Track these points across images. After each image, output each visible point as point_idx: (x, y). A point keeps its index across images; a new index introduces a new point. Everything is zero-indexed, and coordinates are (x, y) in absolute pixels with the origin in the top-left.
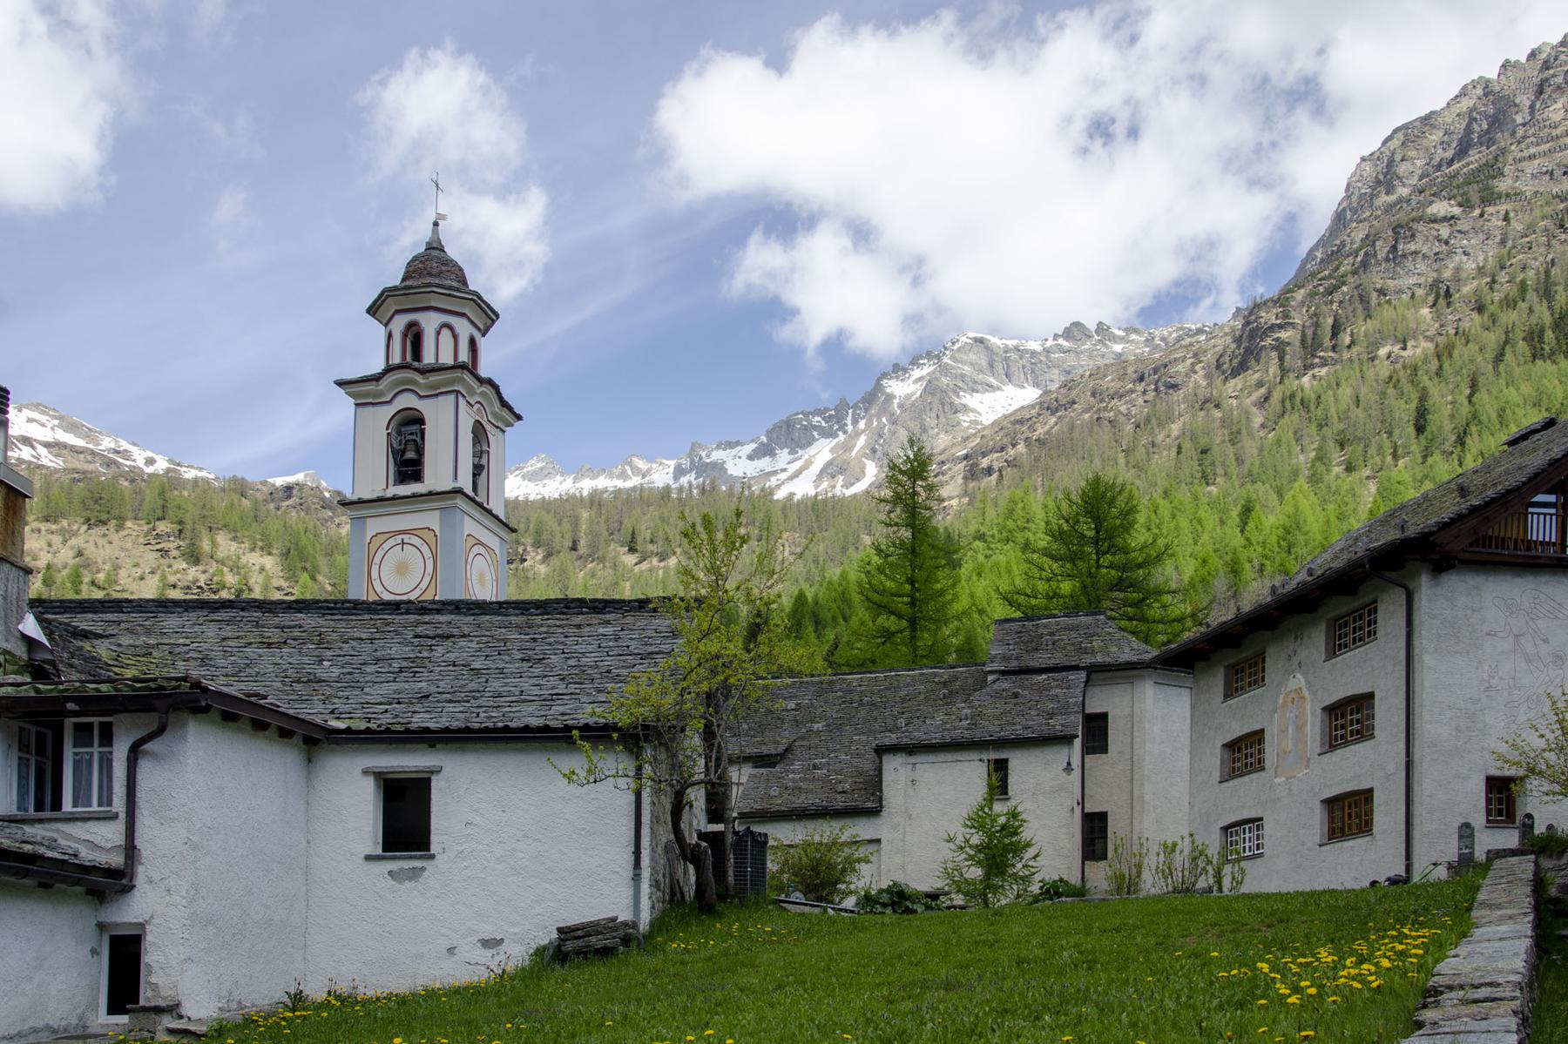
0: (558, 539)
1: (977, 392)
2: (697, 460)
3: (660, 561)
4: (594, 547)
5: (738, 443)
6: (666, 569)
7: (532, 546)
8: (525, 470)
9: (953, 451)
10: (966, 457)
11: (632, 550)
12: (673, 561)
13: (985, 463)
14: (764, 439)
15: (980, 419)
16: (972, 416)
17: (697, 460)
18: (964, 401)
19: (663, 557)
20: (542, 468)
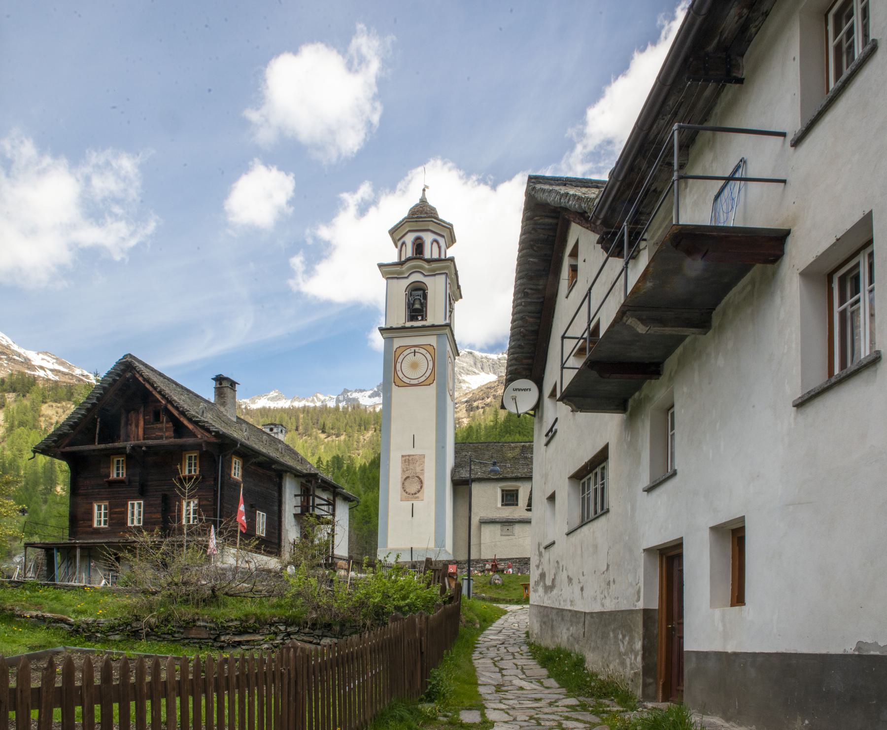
0: (290, 425)
2: (346, 396)
3: (336, 437)
4: (306, 430)
5: (364, 390)
6: (340, 441)
8: (269, 396)
9: (460, 399)
10: (466, 402)
11: (323, 432)
12: (342, 438)
13: (475, 404)
14: (376, 389)
15: (470, 386)
16: (467, 385)
17: (346, 396)
19: (338, 436)
20: (276, 396)
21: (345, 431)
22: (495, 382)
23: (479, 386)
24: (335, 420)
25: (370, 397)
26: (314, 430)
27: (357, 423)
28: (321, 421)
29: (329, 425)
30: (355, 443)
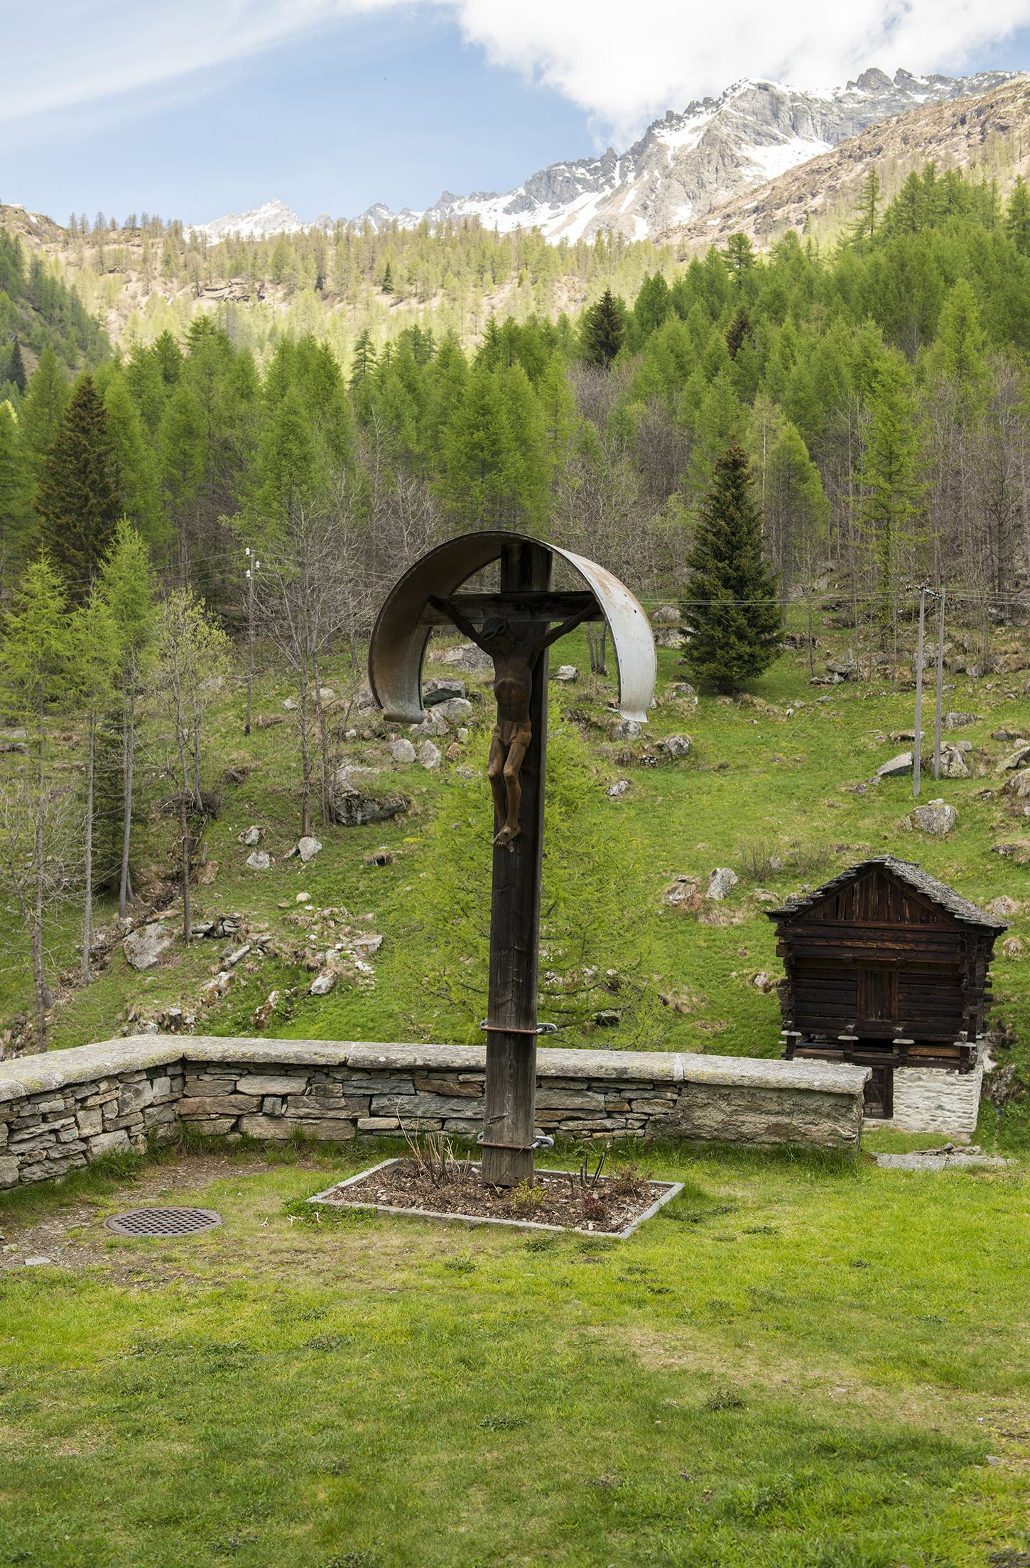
1: (761, 144)
2: (448, 211)
4: (342, 284)
5: (493, 195)
6: (428, 312)
7: (271, 281)
8: (257, 217)
9: (740, 204)
10: (756, 210)
11: (386, 290)
12: (435, 303)
14: (522, 191)
15: (764, 174)
16: (755, 170)
18: (746, 154)
20: (276, 216)
22: (832, 156)
23: (790, 167)
24: (418, 258)
25: (507, 211)
26: (363, 286)
27: (474, 265)
28: (381, 263)
29: (400, 270)
30: (469, 316)
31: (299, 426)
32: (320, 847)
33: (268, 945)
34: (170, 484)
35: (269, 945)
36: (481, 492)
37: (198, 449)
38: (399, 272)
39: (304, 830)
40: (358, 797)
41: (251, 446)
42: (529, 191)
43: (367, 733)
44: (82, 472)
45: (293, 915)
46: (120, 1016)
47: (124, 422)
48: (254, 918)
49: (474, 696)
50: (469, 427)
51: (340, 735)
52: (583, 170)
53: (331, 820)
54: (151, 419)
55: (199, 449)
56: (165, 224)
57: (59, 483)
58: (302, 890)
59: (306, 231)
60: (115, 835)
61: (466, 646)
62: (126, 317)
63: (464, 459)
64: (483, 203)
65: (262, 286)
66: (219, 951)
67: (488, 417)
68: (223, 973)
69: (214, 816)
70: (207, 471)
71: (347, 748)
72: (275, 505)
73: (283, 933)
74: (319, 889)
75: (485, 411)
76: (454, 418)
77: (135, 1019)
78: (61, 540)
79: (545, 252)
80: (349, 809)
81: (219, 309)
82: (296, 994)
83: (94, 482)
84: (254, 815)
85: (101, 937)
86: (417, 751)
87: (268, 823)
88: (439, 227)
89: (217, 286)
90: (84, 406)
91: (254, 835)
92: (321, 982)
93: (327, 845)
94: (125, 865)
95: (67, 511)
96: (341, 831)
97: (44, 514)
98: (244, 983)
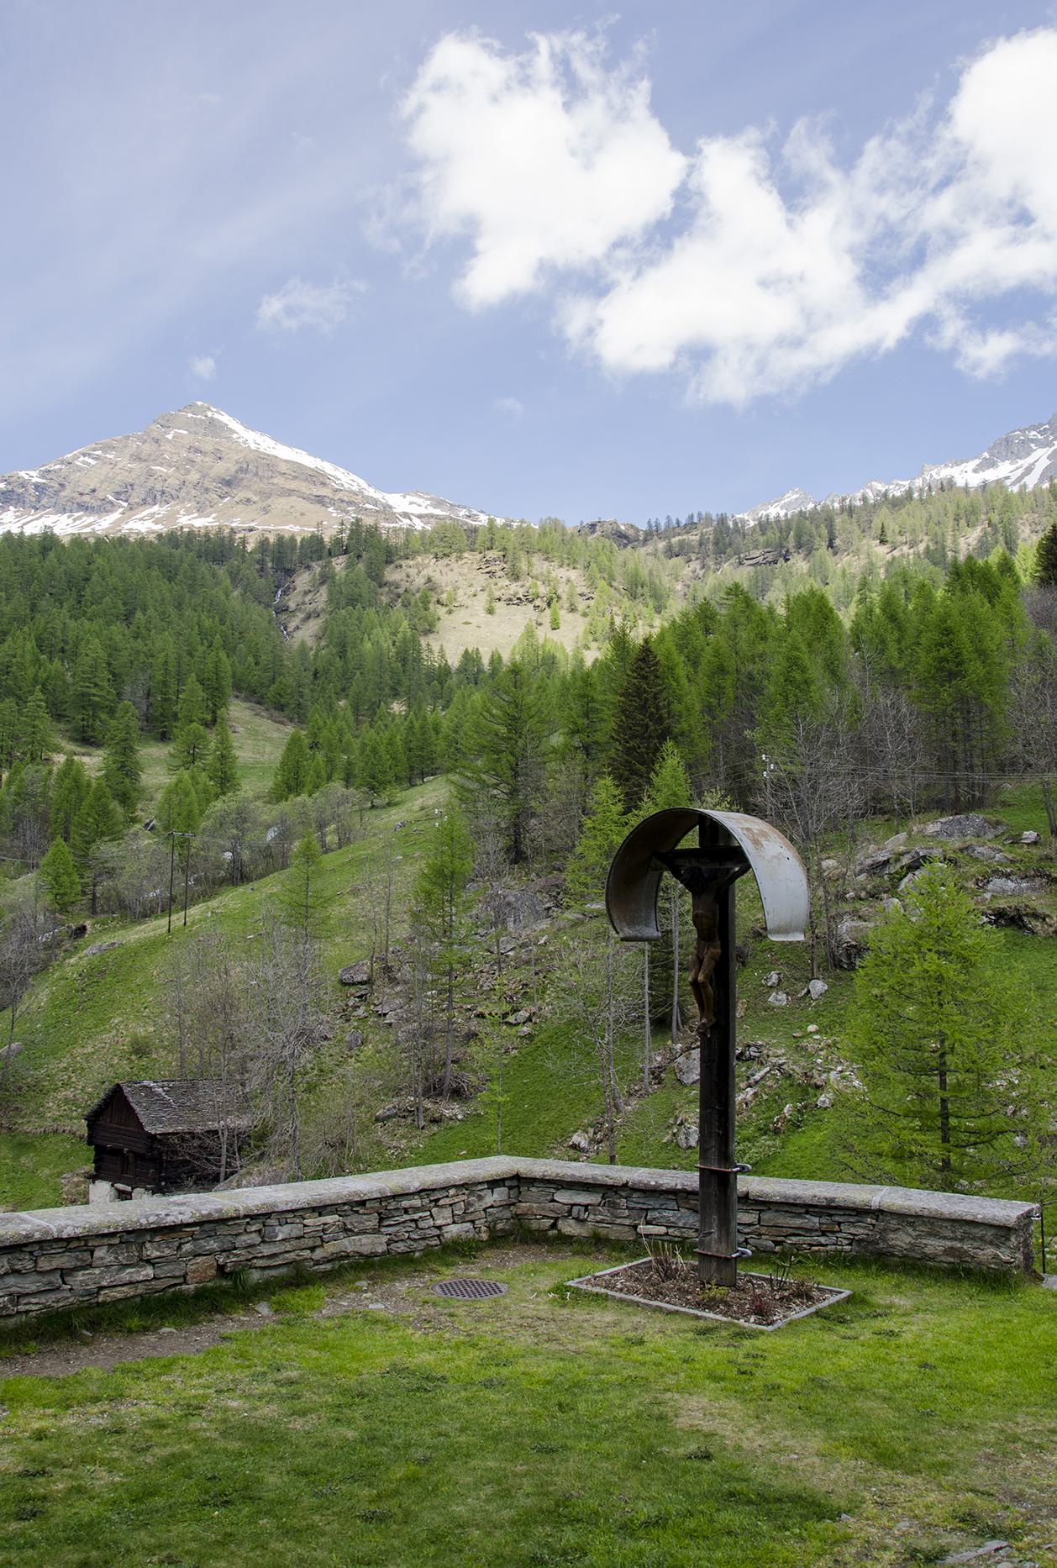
2: (928, 478)
6: (918, 555)
8: (782, 502)
11: (883, 542)
14: (986, 455)
17: (928, 478)
20: (796, 499)
21: (927, 534)
25: (975, 471)
26: (864, 541)
27: (951, 515)
31: (800, 659)
32: (826, 988)
33: (783, 1067)
34: (709, 709)
35: (784, 1067)
36: (950, 695)
37: (728, 682)
38: (891, 529)
39: (813, 975)
40: (855, 946)
41: (768, 676)
42: (991, 455)
43: (863, 894)
44: (643, 708)
45: (804, 1043)
46: (671, 1121)
47: (671, 669)
48: (773, 1045)
49: (950, 861)
50: (936, 645)
51: (841, 897)
52: (1035, 433)
53: (835, 966)
54: (694, 662)
55: (729, 682)
56: (714, 517)
57: (627, 717)
58: (812, 1023)
59: (819, 508)
60: (667, 980)
61: (943, 820)
62: (688, 586)
63: (933, 671)
64: (955, 468)
65: (787, 551)
66: (746, 1071)
67: (951, 636)
68: (749, 1089)
69: (743, 963)
70: (736, 698)
71: (847, 907)
72: (786, 720)
73: (796, 1057)
74: (826, 1021)
75: (948, 632)
76: (923, 640)
77: (682, 1124)
78: (630, 759)
79: (1008, 499)
80: (849, 956)
81: (756, 572)
82: (805, 1107)
83: (652, 714)
84: (774, 963)
85: (659, 1059)
86: (905, 907)
87: (785, 969)
88: (921, 490)
89: (754, 556)
90: (643, 660)
91: (774, 978)
92: (824, 1099)
93: (832, 986)
94: (675, 1003)
95: (633, 737)
96: (844, 975)
97: (617, 740)
98: (765, 1097)
